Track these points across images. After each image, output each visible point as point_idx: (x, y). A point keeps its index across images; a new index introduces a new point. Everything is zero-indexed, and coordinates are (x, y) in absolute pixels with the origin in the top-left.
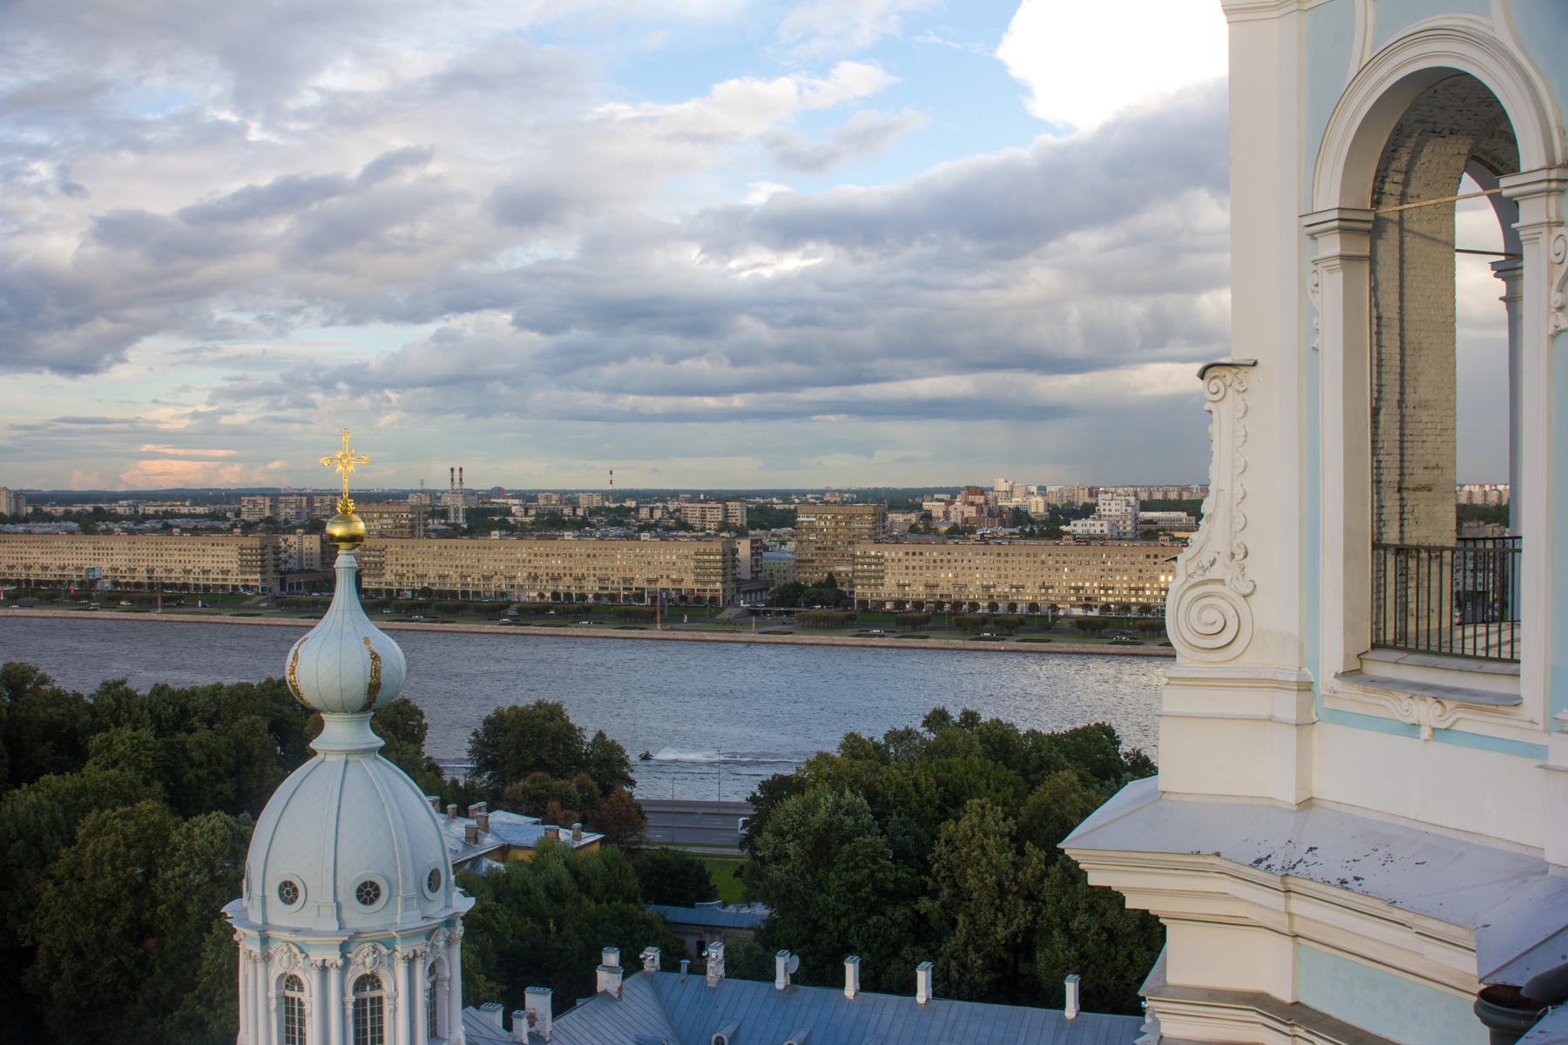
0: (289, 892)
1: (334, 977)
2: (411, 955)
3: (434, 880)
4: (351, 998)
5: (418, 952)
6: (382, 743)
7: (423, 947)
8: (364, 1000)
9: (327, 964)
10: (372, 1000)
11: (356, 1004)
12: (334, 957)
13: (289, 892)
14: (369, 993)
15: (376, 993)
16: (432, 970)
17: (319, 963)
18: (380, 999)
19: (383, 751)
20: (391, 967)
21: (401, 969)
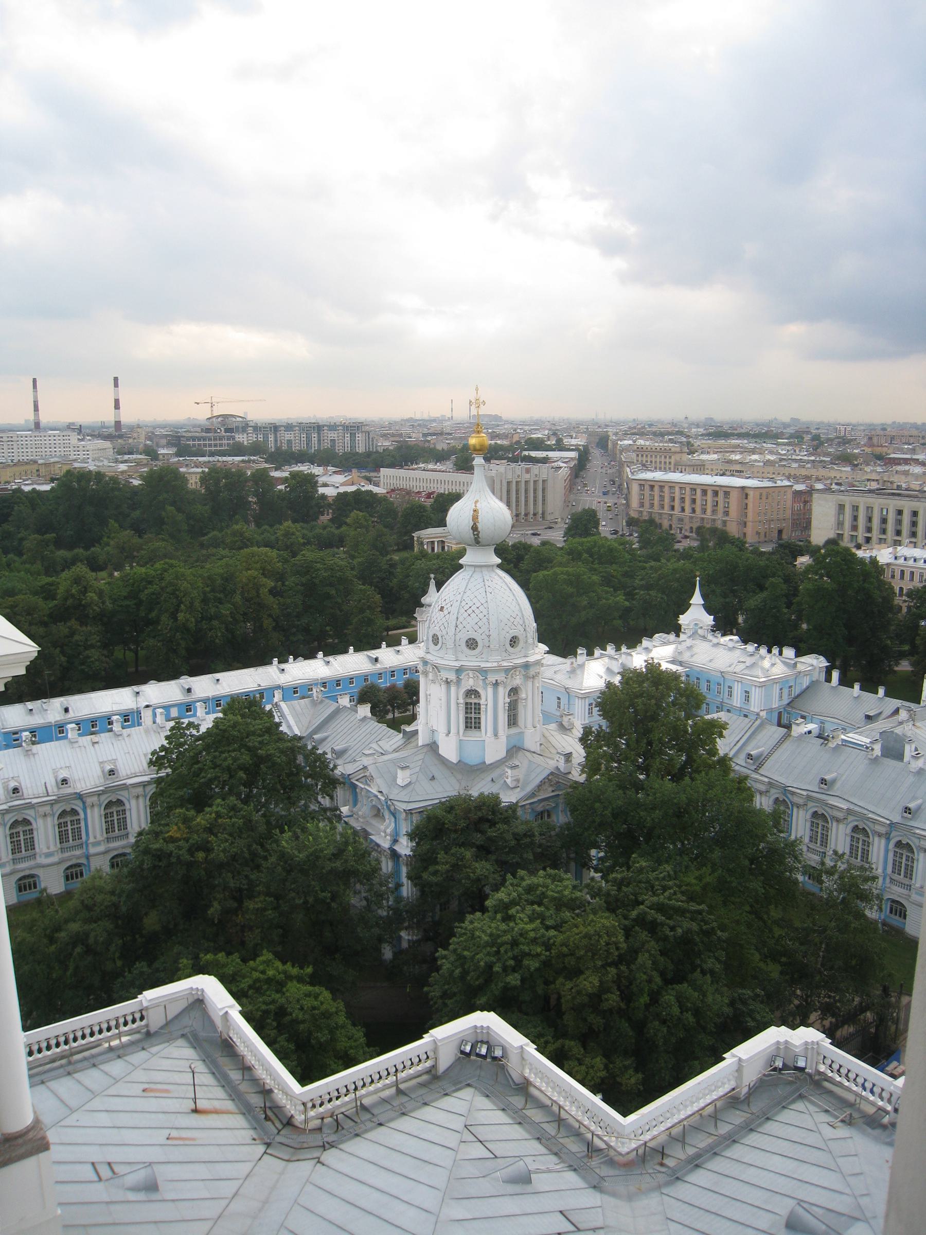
0: (435, 640)
1: (453, 689)
2: (494, 682)
3: (514, 641)
4: (461, 701)
5: (499, 681)
6: (499, 561)
7: (503, 679)
8: (471, 703)
9: (449, 680)
10: (475, 704)
11: (467, 704)
12: (452, 676)
13: (435, 640)
14: (473, 700)
15: (476, 701)
16: (514, 691)
17: (444, 679)
18: (479, 704)
19: (499, 566)
20: (485, 689)
21: (490, 690)
